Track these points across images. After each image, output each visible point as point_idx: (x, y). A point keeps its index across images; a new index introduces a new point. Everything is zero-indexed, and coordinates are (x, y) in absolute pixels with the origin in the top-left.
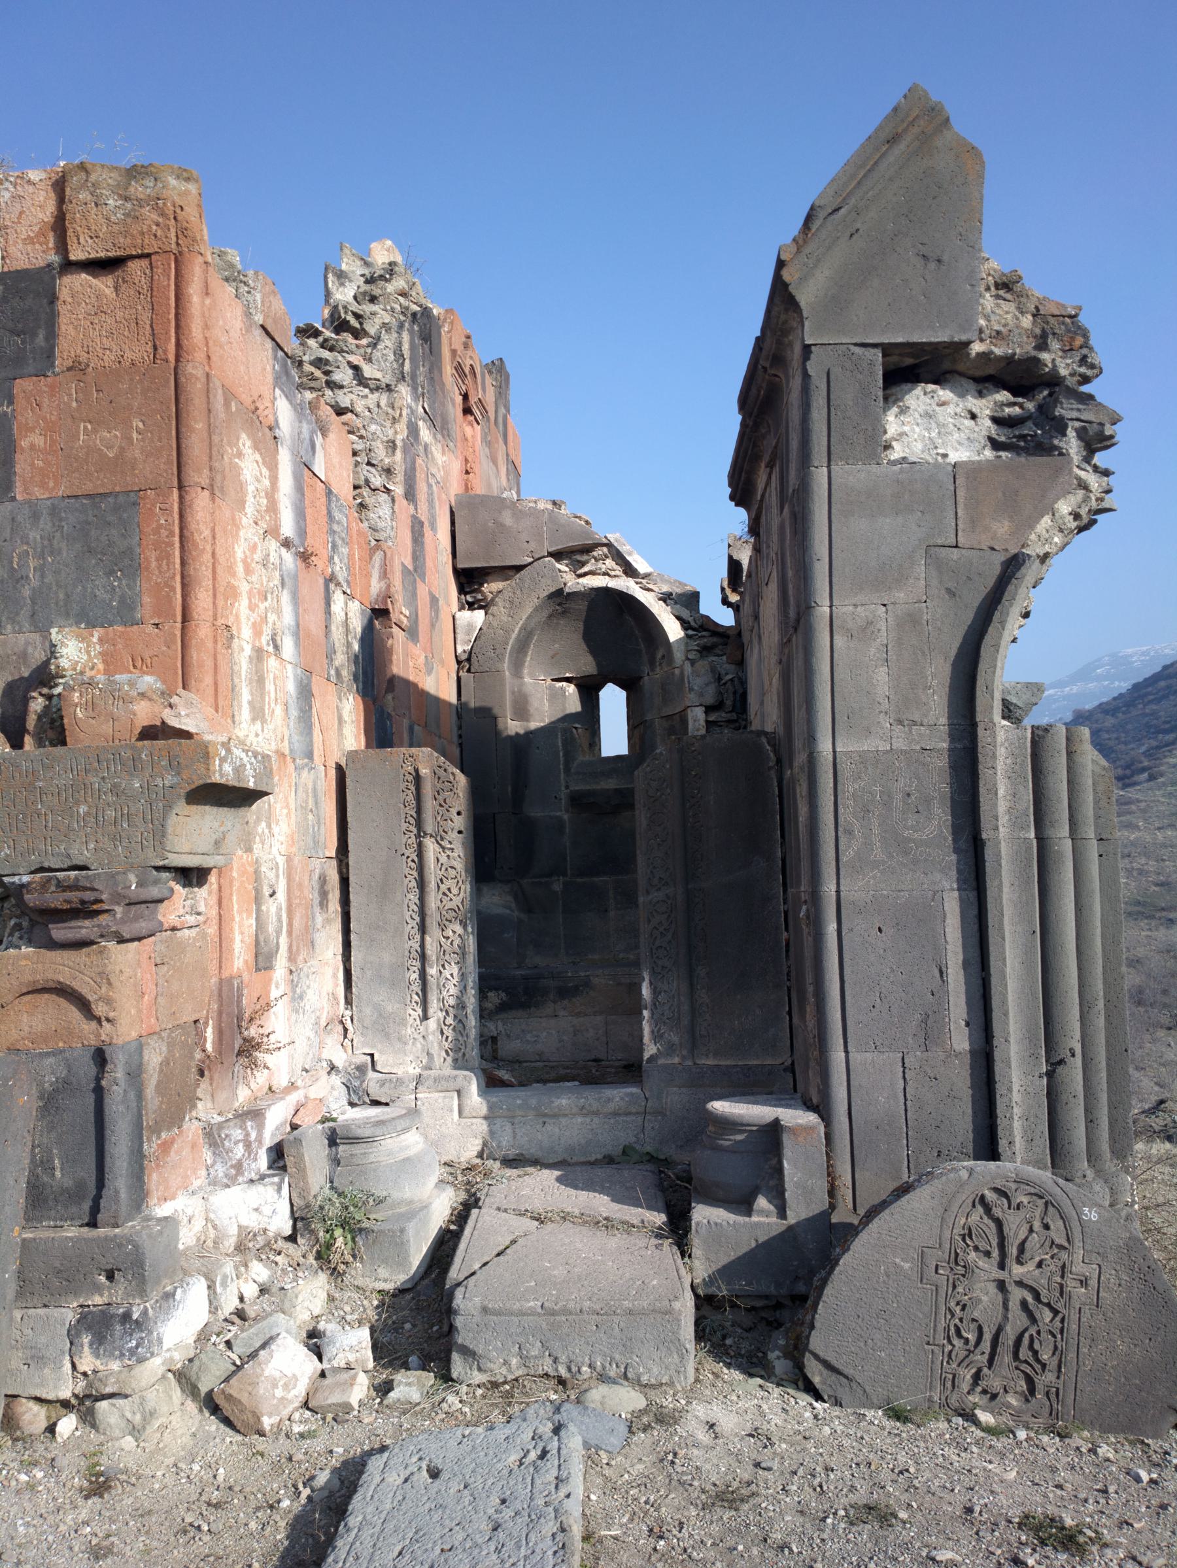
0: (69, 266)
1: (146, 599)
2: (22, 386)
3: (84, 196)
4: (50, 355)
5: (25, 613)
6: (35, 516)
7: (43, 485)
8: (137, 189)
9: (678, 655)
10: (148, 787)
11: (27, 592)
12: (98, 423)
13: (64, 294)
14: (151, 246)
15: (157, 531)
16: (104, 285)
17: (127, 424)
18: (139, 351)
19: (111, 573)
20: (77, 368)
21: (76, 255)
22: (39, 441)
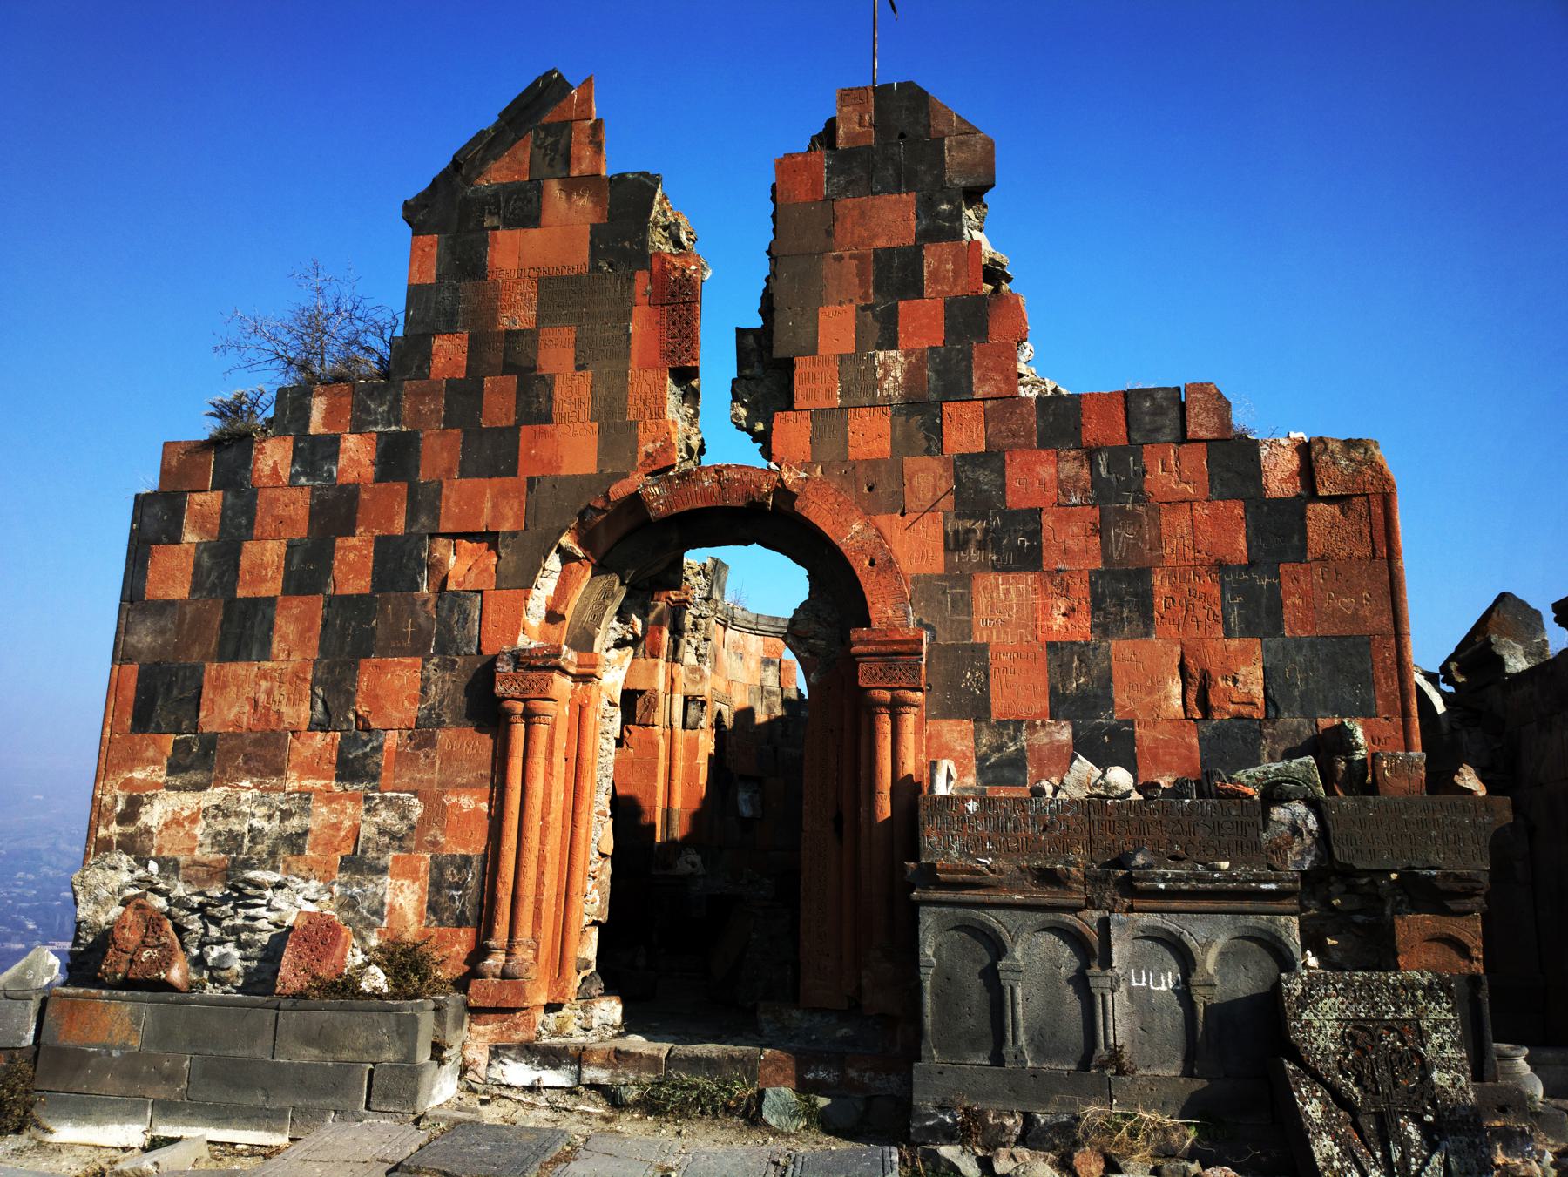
0: (1314, 497)
1: (1379, 702)
2: (1283, 567)
3: (1326, 458)
4: (1303, 549)
5: (1296, 705)
6: (1299, 648)
7: (1303, 628)
8: (1358, 454)
9: (1445, 726)
10: (1473, 823)
11: (1297, 693)
12: (1338, 594)
13: (1310, 514)
14: (1370, 490)
15: (1384, 660)
16: (1334, 510)
17: (1359, 594)
18: (1362, 551)
19: (1354, 684)
20: (1323, 559)
21: (1322, 492)
22: (1299, 602)
